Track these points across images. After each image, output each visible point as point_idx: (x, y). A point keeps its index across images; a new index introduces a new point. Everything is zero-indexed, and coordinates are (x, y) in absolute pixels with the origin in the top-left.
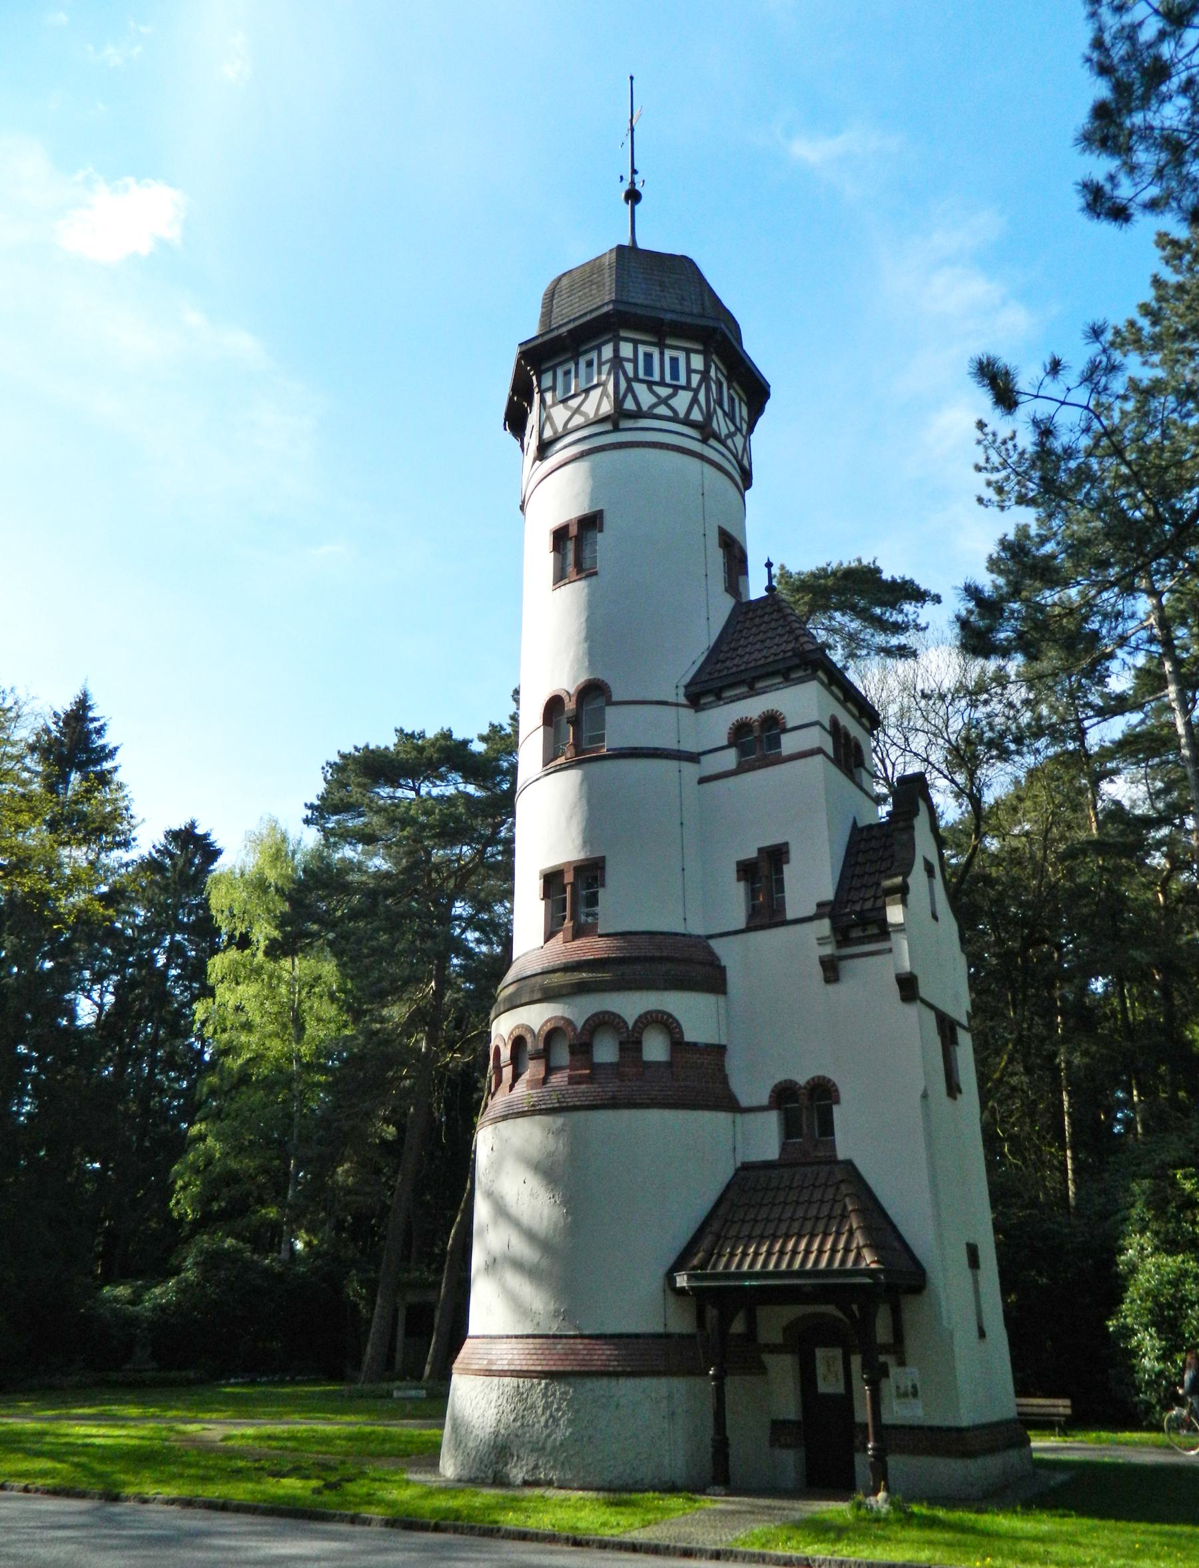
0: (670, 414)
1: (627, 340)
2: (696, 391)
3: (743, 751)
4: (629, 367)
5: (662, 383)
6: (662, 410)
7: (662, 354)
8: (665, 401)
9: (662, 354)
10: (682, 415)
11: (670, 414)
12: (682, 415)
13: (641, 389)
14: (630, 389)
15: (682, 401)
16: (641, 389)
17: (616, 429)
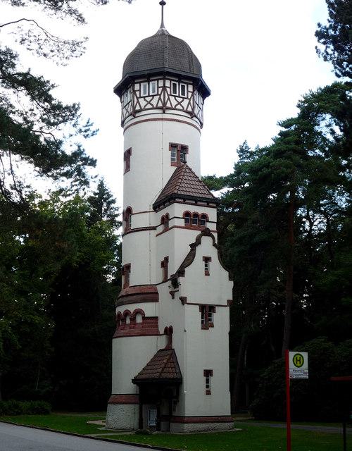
0: (151, 107)
1: (168, 79)
2: (160, 95)
3: (186, 221)
4: (138, 93)
5: (149, 96)
6: (149, 106)
7: (149, 84)
8: (149, 103)
9: (149, 84)
10: (155, 106)
11: (151, 107)
12: (155, 106)
13: (141, 100)
14: (138, 102)
15: (154, 102)
16: (141, 100)
17: (135, 117)
